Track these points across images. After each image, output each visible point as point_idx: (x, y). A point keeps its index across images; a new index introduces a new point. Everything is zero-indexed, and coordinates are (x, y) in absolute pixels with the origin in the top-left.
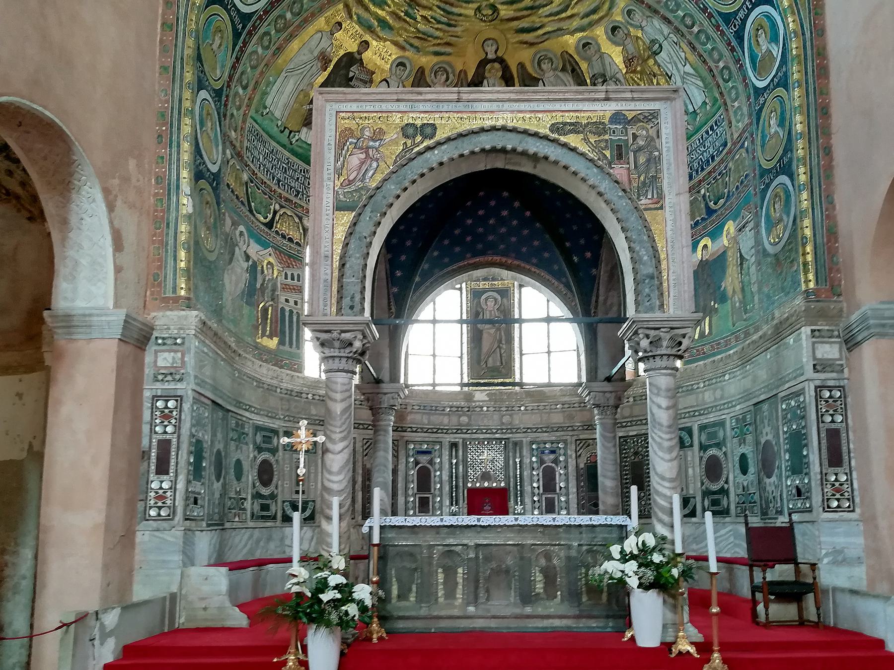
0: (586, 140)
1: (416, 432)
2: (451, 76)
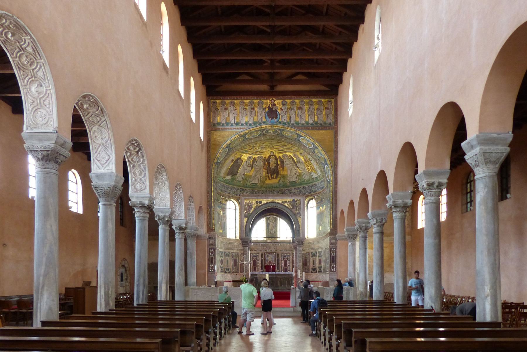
0: (288, 204)
1: (253, 251)
2: (262, 158)
